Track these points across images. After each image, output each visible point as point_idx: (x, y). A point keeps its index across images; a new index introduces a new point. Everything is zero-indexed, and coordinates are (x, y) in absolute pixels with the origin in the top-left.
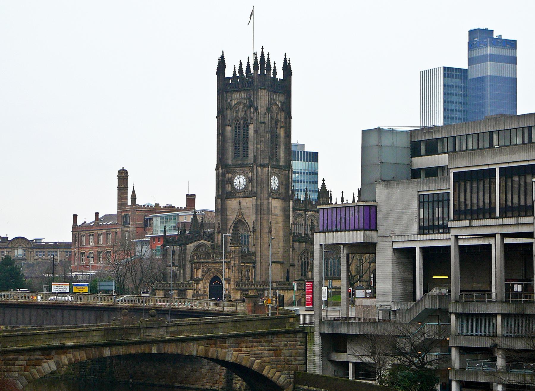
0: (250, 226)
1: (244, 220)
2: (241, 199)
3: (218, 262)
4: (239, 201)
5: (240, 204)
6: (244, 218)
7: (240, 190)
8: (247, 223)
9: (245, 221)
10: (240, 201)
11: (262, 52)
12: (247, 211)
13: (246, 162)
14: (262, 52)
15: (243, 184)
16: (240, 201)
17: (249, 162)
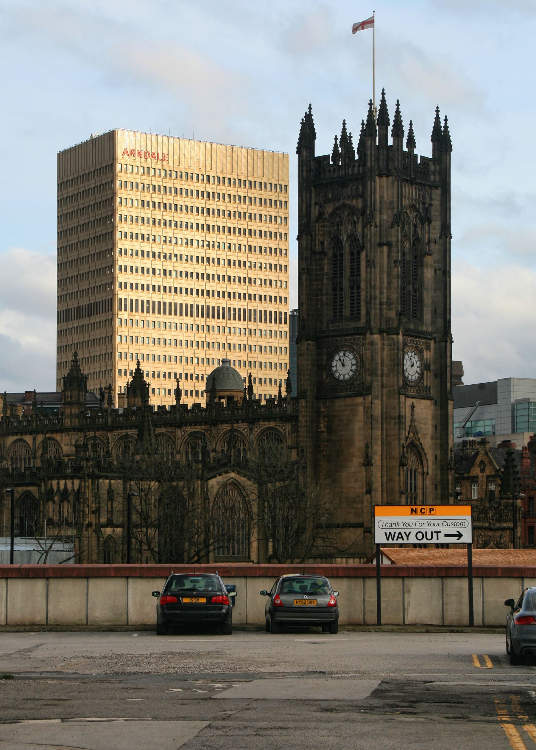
0: (427, 455)
1: (419, 444)
2: (414, 400)
3: (498, 529)
4: (411, 403)
5: (413, 411)
6: (419, 439)
7: (412, 382)
8: (423, 449)
9: (421, 445)
10: (413, 403)
11: (437, 118)
12: (422, 426)
13: (420, 329)
14: (437, 118)
15: (417, 372)
16: (413, 403)
17: (424, 329)
